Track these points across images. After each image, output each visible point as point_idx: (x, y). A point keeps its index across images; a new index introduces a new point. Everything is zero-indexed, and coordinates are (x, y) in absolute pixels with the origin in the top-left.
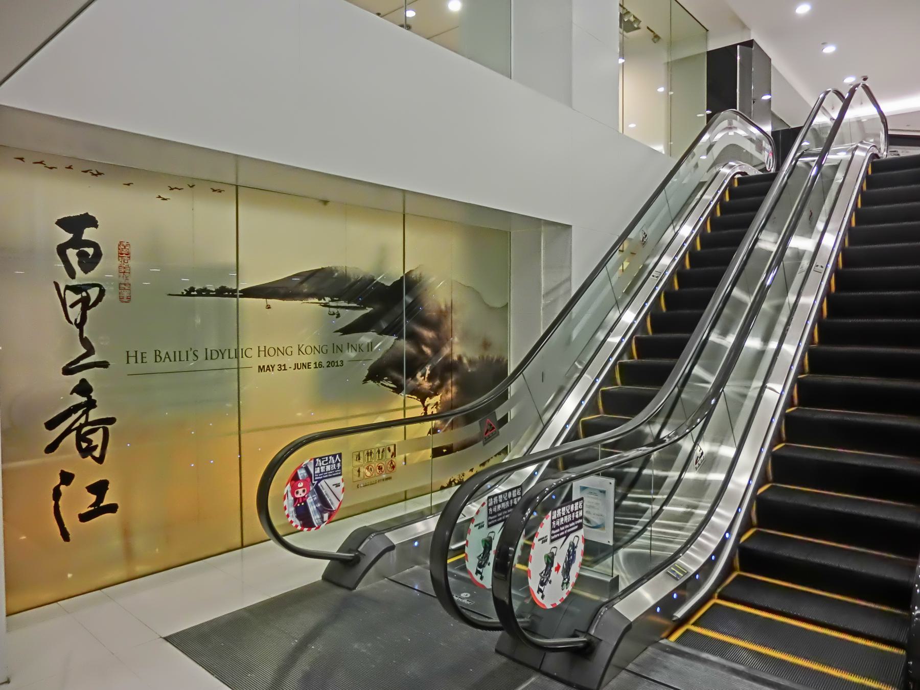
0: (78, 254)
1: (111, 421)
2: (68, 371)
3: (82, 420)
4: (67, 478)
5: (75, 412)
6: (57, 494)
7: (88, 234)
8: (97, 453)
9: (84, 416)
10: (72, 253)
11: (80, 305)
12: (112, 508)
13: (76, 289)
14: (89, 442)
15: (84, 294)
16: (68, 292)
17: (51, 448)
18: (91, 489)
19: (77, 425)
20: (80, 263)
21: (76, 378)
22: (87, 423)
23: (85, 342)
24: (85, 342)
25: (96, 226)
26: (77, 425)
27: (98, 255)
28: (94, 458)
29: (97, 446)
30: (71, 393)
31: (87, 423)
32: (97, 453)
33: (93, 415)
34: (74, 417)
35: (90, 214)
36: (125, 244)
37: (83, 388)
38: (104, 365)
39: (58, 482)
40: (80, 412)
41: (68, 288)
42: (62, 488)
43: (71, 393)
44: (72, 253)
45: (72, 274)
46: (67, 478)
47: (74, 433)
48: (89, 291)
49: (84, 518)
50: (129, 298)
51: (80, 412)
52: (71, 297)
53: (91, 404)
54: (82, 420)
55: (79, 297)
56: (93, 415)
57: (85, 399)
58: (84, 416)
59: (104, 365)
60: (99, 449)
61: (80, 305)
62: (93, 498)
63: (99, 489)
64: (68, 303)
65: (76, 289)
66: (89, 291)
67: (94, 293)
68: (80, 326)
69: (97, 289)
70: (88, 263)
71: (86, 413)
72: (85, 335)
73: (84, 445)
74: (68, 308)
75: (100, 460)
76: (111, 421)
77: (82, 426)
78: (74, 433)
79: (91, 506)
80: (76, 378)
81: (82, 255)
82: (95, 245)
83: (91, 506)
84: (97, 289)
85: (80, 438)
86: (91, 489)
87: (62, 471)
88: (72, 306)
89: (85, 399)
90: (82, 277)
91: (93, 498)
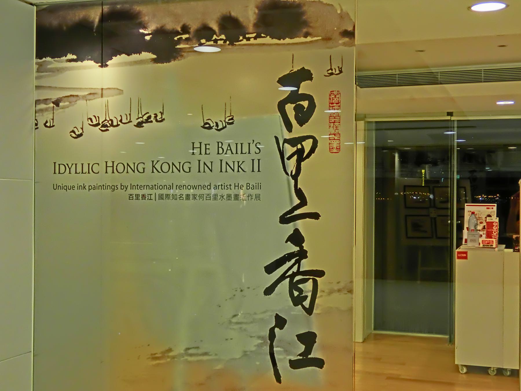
0: (295, 109)
1: (321, 274)
2: (285, 219)
3: (295, 269)
4: (280, 322)
5: (289, 260)
6: (272, 336)
7: (305, 88)
8: (307, 303)
9: (297, 265)
10: (290, 108)
11: (295, 157)
12: (319, 363)
13: (292, 142)
14: (301, 291)
15: (299, 146)
16: (286, 144)
17: (269, 291)
18: (301, 338)
19: (290, 273)
20: (296, 117)
21: (289, 229)
22: (299, 273)
23: (299, 193)
24: (299, 193)
25: (311, 79)
26: (290, 273)
27: (312, 106)
28: (303, 307)
29: (306, 297)
30: (286, 242)
31: (299, 273)
32: (307, 303)
33: (306, 265)
34: (288, 264)
35: (306, 68)
36: (335, 93)
37: (296, 238)
38: (315, 216)
39: (273, 324)
40: (293, 261)
41: (286, 141)
42: (277, 330)
43: (286, 242)
44: (290, 108)
45: (289, 127)
46: (280, 322)
47: (288, 279)
48: (303, 143)
49: (294, 365)
50: (339, 149)
51: (293, 261)
52: (289, 150)
53: (302, 254)
54: (295, 269)
55: (295, 149)
56: (306, 265)
57: (297, 249)
58: (297, 265)
59: (315, 216)
60: (309, 299)
61: (295, 157)
62: (302, 348)
63: (308, 339)
64: (287, 156)
65: (292, 142)
66: (303, 143)
67: (307, 145)
68: (295, 177)
69: (311, 141)
70: (303, 117)
71: (298, 262)
72: (299, 187)
73: (296, 293)
74: (286, 160)
75: (309, 311)
76: (321, 274)
77: (294, 275)
78: (288, 280)
79: (300, 355)
80: (289, 229)
81: (298, 109)
82: (310, 98)
83: (300, 355)
84: (311, 141)
85: (293, 286)
86: (301, 338)
87: (277, 314)
88: (289, 158)
89: (297, 249)
90: (298, 131)
91: (302, 348)
